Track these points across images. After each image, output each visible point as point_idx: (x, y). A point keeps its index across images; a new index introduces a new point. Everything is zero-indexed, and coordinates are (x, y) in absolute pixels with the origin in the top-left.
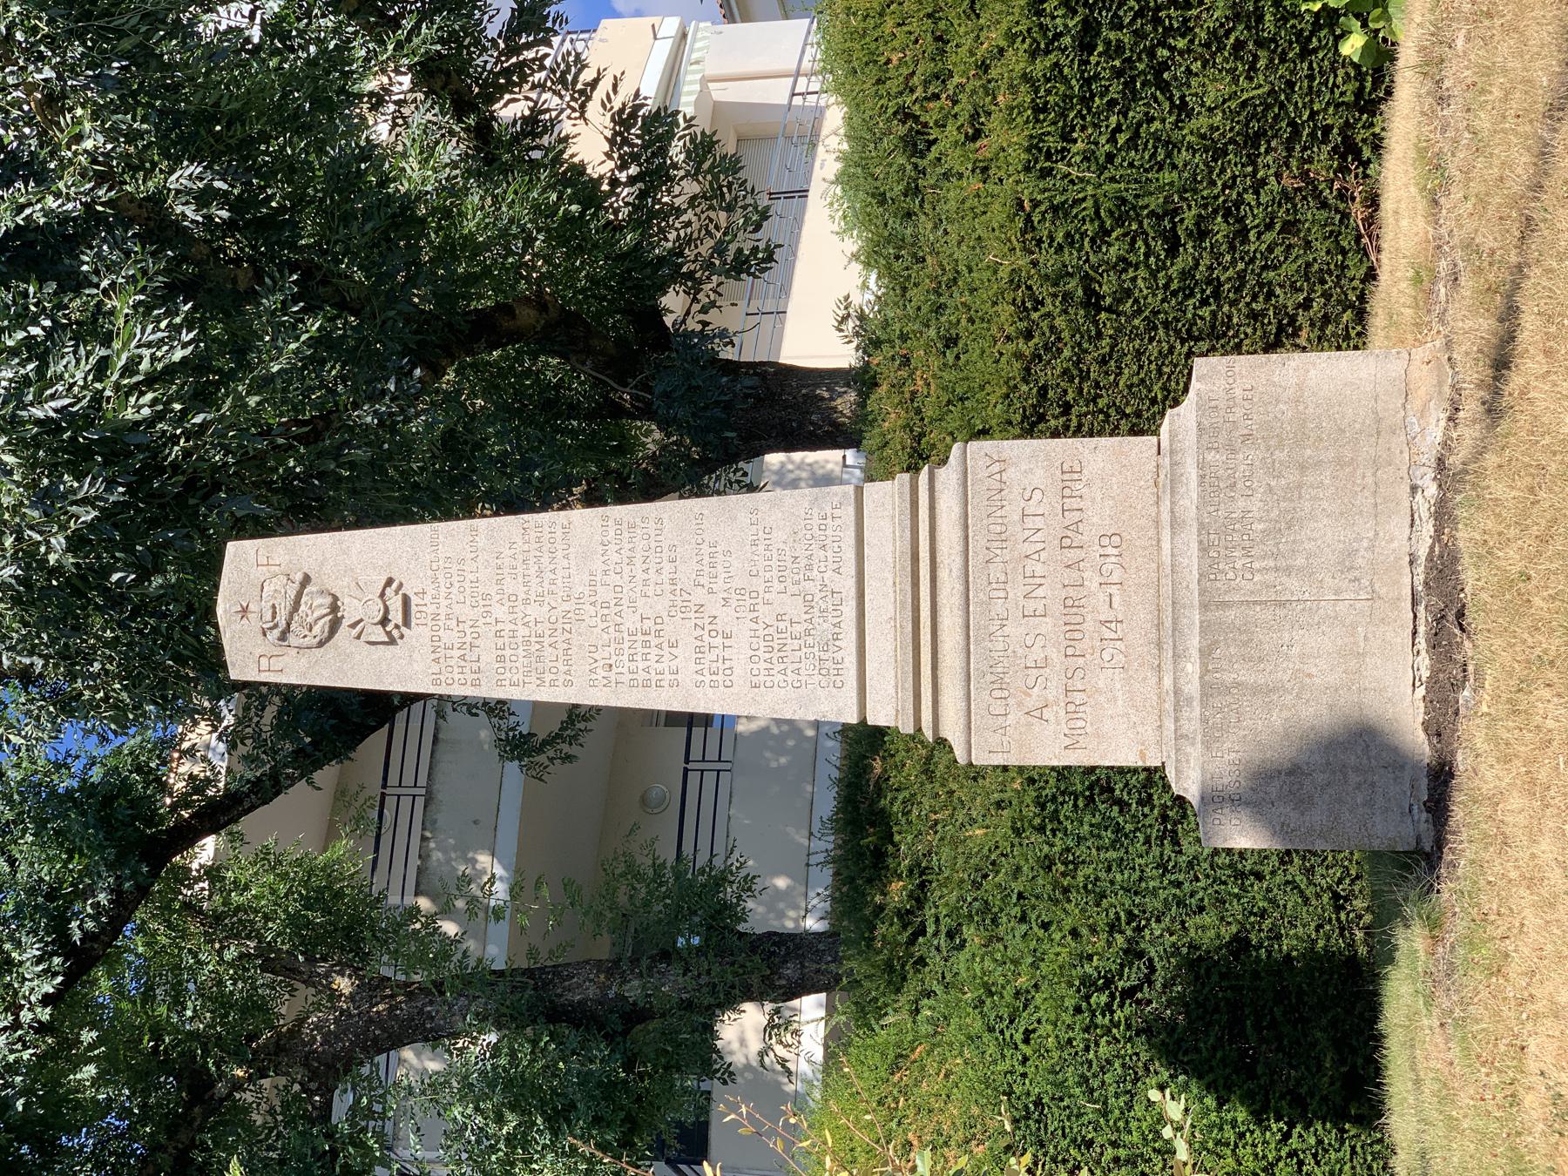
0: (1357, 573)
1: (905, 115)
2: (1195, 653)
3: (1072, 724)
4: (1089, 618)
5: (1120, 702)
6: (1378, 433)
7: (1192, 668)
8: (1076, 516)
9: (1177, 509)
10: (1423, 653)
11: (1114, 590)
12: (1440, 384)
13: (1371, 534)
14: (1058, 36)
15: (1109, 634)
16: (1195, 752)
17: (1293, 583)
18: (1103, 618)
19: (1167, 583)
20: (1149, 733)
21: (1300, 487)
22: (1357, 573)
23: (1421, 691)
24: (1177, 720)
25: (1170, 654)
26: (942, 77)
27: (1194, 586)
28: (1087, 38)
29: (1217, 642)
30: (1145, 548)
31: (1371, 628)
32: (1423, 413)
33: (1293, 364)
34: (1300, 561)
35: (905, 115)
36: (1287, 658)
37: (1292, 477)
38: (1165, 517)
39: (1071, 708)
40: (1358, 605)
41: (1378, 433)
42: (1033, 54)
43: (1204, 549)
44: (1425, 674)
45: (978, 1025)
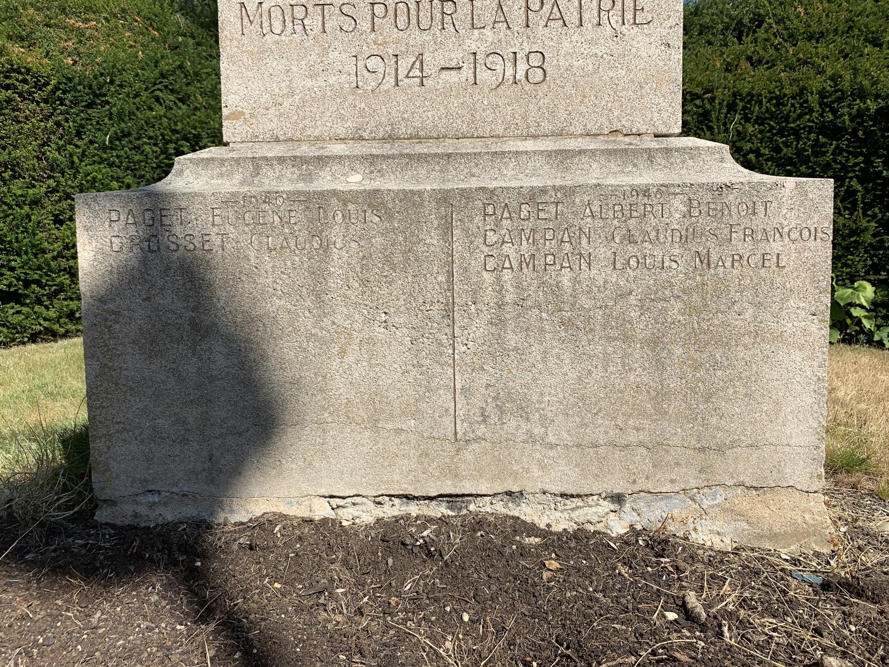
0: (494, 419)
1: (759, 21)
2: (377, 184)
3: (276, 13)
4: (427, 36)
5: (309, 83)
6: (702, 450)
7: (354, 180)
8: (572, 18)
9: (585, 159)
10: (379, 512)
11: (467, 72)
12: (774, 537)
13: (551, 439)
14: (834, 111)
15: (404, 65)
16: (229, 185)
17: (479, 328)
18: (427, 57)
19: (478, 146)
20: (269, 124)
21: (626, 338)
22: (494, 419)
23: (321, 510)
24: (281, 160)
25: (374, 151)
26: (792, 38)
27: (474, 183)
28: (833, 131)
29: (390, 217)
30: (525, 118)
31: (413, 438)
32: (731, 512)
33: (814, 328)
34: (512, 339)
35: (759, 21)
36: (369, 321)
37: (641, 328)
38: (572, 144)
39: (299, 12)
40: (448, 421)
41: (702, 450)
42: (822, 94)
43: (534, 196)
44: (346, 516)
45: (164, 66)
